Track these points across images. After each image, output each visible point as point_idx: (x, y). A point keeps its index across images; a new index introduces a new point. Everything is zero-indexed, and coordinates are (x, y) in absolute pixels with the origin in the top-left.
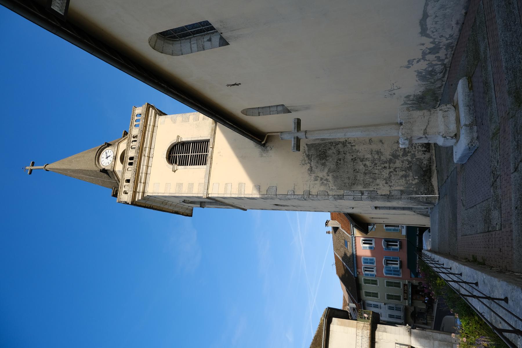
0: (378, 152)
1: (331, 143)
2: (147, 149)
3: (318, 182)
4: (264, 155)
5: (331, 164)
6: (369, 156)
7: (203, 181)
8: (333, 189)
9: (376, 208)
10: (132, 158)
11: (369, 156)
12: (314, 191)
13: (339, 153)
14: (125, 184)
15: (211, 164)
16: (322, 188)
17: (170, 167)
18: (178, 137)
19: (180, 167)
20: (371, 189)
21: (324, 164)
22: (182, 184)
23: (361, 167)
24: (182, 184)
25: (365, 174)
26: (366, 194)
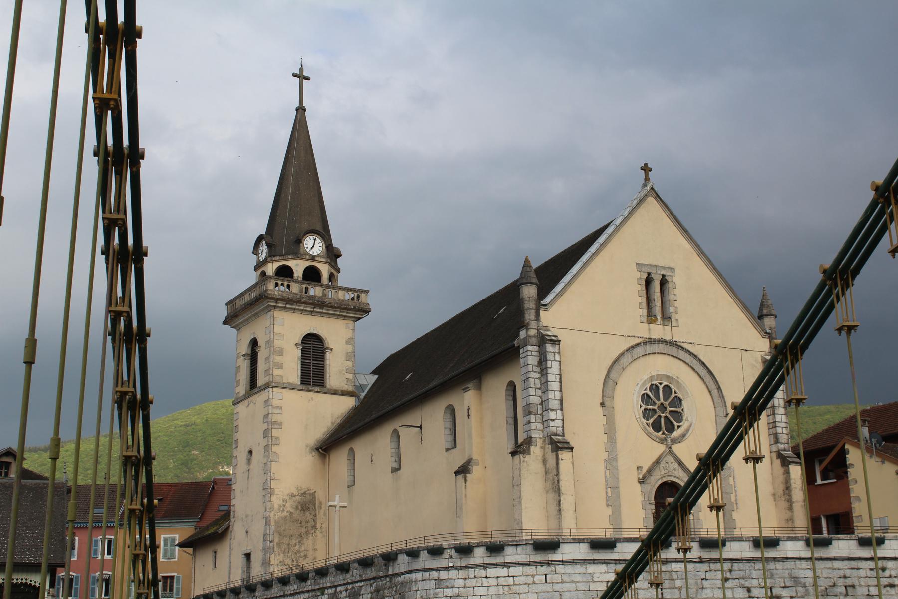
0: (306, 556)
1: (315, 515)
3: (281, 503)
5: (297, 514)
7: (285, 381)
8: (275, 516)
9: (248, 556)
12: (274, 498)
14: (286, 283)
16: (276, 506)
18: (331, 349)
19: (300, 351)
20: (276, 549)
21: (297, 508)
23: (294, 541)
25: (288, 544)
26: (271, 544)
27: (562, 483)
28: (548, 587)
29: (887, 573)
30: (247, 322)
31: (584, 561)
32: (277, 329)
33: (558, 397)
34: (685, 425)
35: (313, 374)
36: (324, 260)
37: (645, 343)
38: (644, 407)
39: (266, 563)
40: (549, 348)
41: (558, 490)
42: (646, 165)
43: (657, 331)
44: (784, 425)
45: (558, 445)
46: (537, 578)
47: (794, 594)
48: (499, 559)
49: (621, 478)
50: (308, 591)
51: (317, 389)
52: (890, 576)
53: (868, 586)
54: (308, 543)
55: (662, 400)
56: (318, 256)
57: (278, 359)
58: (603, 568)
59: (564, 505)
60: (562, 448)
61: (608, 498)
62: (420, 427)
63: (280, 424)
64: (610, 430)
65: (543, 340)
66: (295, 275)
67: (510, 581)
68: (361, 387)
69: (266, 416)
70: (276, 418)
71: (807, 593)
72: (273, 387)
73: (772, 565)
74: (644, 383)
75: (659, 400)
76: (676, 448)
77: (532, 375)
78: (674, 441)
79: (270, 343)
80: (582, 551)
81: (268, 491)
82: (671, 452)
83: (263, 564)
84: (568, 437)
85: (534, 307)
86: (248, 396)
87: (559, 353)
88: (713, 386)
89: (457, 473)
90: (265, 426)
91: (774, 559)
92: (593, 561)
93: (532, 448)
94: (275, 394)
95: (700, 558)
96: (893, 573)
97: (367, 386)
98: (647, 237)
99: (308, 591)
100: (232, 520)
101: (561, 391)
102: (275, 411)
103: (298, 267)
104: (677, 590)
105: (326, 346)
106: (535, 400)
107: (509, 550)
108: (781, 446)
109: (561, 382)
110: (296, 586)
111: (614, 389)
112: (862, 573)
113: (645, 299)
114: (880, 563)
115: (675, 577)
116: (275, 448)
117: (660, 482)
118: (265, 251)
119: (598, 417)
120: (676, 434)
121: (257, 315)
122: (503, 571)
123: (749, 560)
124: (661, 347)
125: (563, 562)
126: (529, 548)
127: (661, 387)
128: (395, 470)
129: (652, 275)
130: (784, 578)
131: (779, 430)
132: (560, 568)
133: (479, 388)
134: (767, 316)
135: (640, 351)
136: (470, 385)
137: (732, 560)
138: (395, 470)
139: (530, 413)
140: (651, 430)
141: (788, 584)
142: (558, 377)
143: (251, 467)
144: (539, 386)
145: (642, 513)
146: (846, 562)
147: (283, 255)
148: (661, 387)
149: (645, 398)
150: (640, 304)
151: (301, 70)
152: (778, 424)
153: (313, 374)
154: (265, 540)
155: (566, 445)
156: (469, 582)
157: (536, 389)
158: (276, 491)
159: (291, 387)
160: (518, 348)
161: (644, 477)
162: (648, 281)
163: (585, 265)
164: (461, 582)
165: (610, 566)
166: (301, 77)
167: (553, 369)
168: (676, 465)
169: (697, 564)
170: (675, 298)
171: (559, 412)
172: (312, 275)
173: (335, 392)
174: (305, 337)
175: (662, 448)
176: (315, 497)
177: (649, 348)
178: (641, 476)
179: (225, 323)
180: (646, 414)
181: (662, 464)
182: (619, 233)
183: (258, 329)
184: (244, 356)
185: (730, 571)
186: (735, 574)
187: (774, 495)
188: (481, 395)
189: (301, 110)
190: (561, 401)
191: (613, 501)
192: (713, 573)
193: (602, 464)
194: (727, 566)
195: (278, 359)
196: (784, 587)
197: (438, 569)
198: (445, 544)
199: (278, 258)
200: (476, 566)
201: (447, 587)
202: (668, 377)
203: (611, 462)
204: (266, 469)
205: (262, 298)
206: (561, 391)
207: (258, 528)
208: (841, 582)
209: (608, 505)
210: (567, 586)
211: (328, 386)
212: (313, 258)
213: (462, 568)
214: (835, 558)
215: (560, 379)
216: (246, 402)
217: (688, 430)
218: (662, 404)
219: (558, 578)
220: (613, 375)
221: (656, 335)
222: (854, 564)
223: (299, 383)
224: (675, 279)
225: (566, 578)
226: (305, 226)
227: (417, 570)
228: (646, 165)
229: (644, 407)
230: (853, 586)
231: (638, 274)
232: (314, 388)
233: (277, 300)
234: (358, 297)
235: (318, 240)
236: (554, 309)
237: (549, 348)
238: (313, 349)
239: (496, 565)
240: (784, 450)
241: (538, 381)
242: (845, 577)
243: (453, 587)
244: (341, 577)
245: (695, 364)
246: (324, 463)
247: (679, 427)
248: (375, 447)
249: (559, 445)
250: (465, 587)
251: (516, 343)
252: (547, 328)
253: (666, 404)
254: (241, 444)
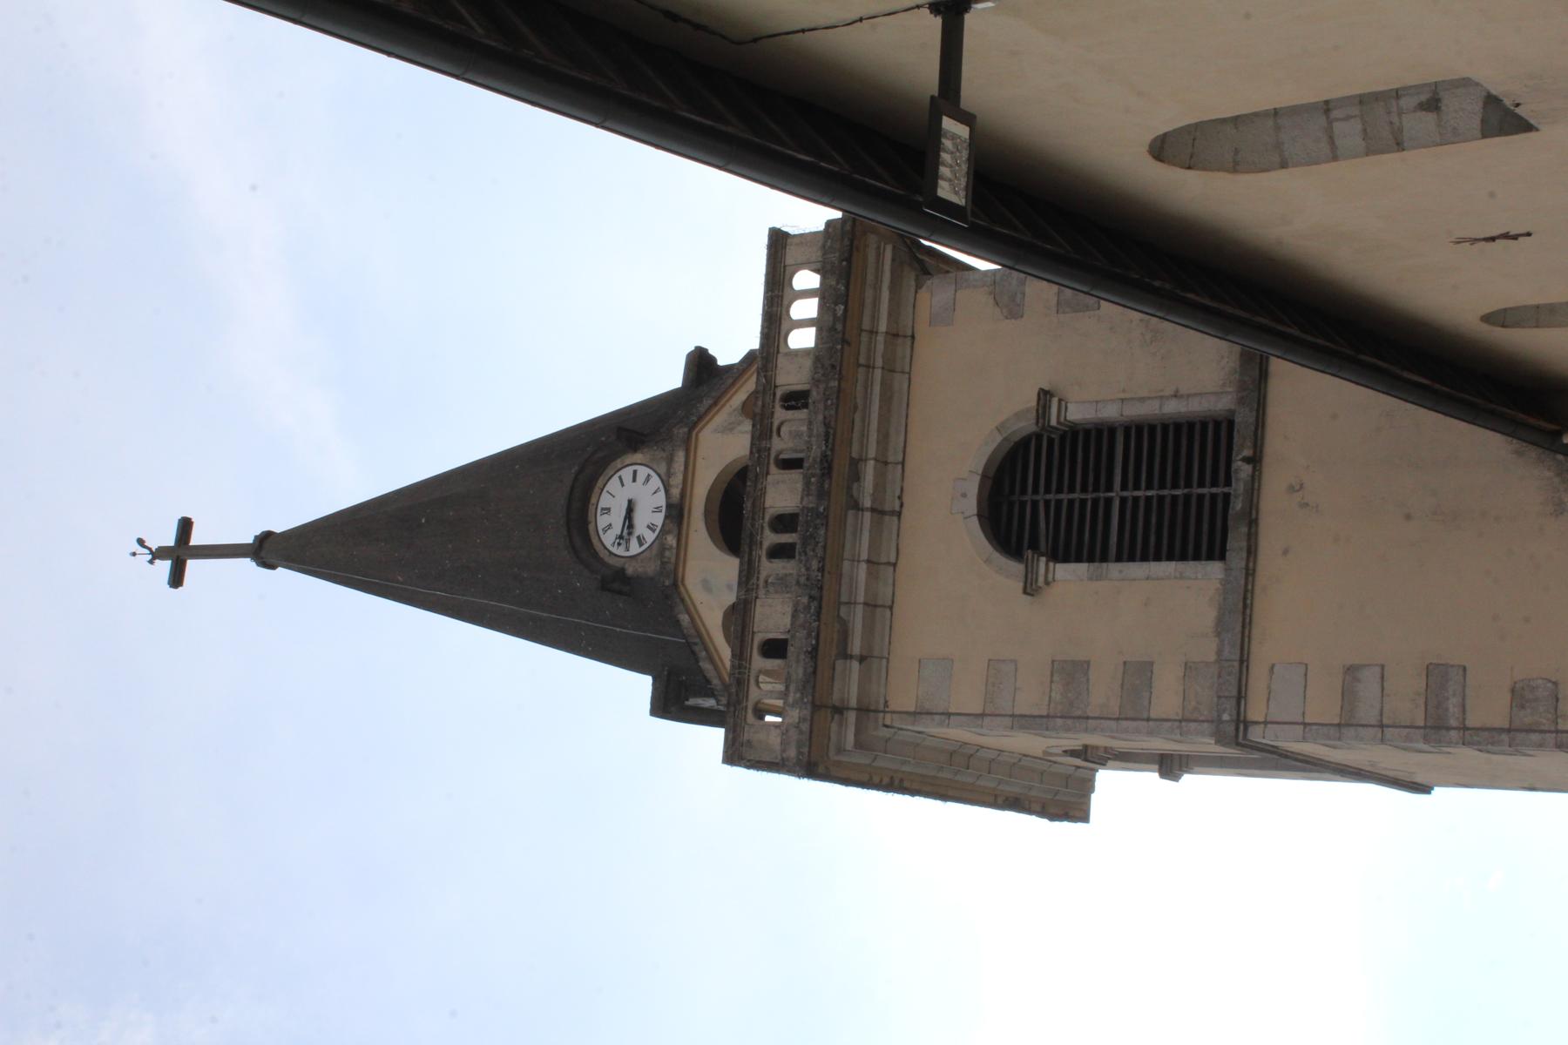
2: (869, 470)
7: (1207, 650)
10: (784, 522)
15: (1252, 552)
17: (1005, 574)
18: (1045, 396)
19: (1063, 571)
22: (1084, 666)
24: (1084, 666)
36: (680, 457)
105: (1028, 426)
151: (158, 554)
159: (1239, 614)
166: (180, 553)
189: (269, 550)
211: (1222, 404)
212: (676, 513)
223: (1215, 569)
232: (1238, 488)
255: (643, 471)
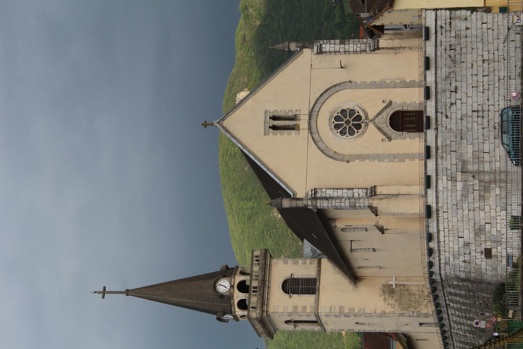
0: (422, 291)
2: (267, 282)
3: (390, 306)
4: (356, 289)
5: (397, 297)
6: (417, 293)
7: (314, 305)
8: (398, 310)
10: (254, 288)
11: (417, 293)
12: (387, 311)
13: (401, 290)
16: (392, 310)
17: (287, 296)
18: (292, 274)
19: (294, 295)
20: (418, 310)
21: (393, 296)
22: (297, 307)
23: (413, 299)
24: (297, 307)
25: (415, 302)
26: (415, 313)
27: (394, 193)
28: (450, 211)
29: (444, 25)
30: (273, 325)
31: (436, 192)
32: (281, 310)
33: (345, 191)
34: (357, 109)
35: (307, 286)
36: (233, 279)
37: (311, 133)
38: (347, 134)
39: (426, 315)
40: (319, 195)
41: (397, 195)
42: (203, 125)
43: (303, 123)
44: (355, 46)
45: (372, 192)
46: (445, 217)
47: (454, 79)
48: (435, 235)
49: (388, 152)
50: (447, 310)
51: (318, 284)
52: (445, 24)
53: (450, 37)
54: (414, 290)
55: (343, 122)
56: (230, 283)
57: (300, 310)
58: (440, 182)
59: (406, 193)
60: (375, 192)
61: (400, 161)
62: (351, 241)
63: (341, 307)
64: (362, 157)
65: (315, 198)
66: (244, 298)
67: (446, 230)
68: (313, 251)
69: (336, 316)
70: (337, 310)
71: (454, 72)
72: (318, 313)
73: (439, 90)
74: (333, 132)
75: (343, 124)
76: (371, 117)
77: (333, 204)
78: (367, 118)
79: (289, 314)
80: (431, 193)
81: (383, 314)
82: (372, 120)
83: (427, 317)
84: (369, 187)
85: (295, 201)
86: (321, 325)
87: (321, 189)
88: (334, 90)
89: (383, 233)
90: (342, 317)
91: (436, 88)
92: (436, 187)
93: (374, 206)
94: (323, 310)
95: (435, 129)
96: (444, 22)
97: (312, 247)
98: (246, 124)
99: (447, 310)
100: (398, 332)
101: (342, 189)
102: (333, 311)
103: (238, 296)
104: (452, 143)
105: (289, 277)
106: (347, 203)
107: (431, 230)
108: (368, 49)
109: (337, 189)
110: (444, 314)
111: (339, 154)
112: (443, 40)
113: (285, 131)
114: (439, 29)
115: (444, 144)
116: (356, 311)
117: (390, 127)
118: (227, 316)
119: (355, 164)
120: (362, 114)
121: (270, 321)
122: (442, 233)
123: (436, 103)
124: (313, 122)
125: (437, 203)
126: (430, 220)
127: (336, 123)
128: (366, 230)
129: (271, 125)
130: (446, 84)
131: (358, 49)
132: (440, 204)
133: (334, 220)
134: (289, 48)
135: (316, 136)
136: (333, 225)
137: (436, 112)
138: (366, 230)
139: (355, 206)
140: (360, 131)
141: (449, 82)
142: (335, 190)
143: (366, 323)
144: (340, 200)
145: (408, 140)
146: (438, 48)
147: (231, 306)
148: (336, 123)
149: (342, 133)
150: (288, 134)
151: (99, 292)
152: (355, 50)
153: (307, 286)
154: (413, 317)
155: (373, 190)
156: (447, 250)
157: (341, 202)
158: (383, 310)
159: (317, 301)
160: (318, 209)
161: (388, 138)
162: (274, 128)
163: (268, 169)
164: (447, 254)
165: (439, 178)
166: (104, 292)
167: (330, 193)
168: (380, 116)
169: (439, 131)
170: (283, 111)
171: (354, 191)
172: (243, 287)
173: (319, 272)
174: (284, 292)
175: (371, 125)
176: (386, 285)
177: (314, 130)
178: (387, 140)
179: (272, 338)
180: (352, 133)
181: (380, 125)
182: (247, 145)
183: (279, 322)
184: (295, 327)
185: (442, 113)
186: (444, 111)
187: (395, 53)
188: (338, 219)
189: (128, 292)
190: (348, 189)
191: (401, 157)
192: (443, 123)
193: (381, 163)
194: (439, 115)
195: (300, 310)
196: (451, 84)
197: (440, 264)
198: (427, 260)
199: (233, 309)
200: (439, 246)
201: (449, 260)
202: (331, 117)
203: (380, 158)
204: (370, 315)
205: (262, 321)
206: (342, 189)
207: (405, 320)
208: (448, 52)
209: (404, 161)
210: (449, 201)
211: (315, 277)
212: (232, 286)
213: (439, 253)
214: (436, 54)
215: (336, 189)
216: (325, 326)
217: (360, 108)
218: (345, 122)
219: (445, 206)
220: (331, 154)
221: (306, 126)
222: (439, 44)
223: (314, 295)
224: (272, 111)
225: (445, 202)
226: (210, 291)
227: (440, 272)
228: (203, 125)
229: (347, 134)
230: (451, 45)
231: (271, 135)
232: (317, 286)
233: (263, 311)
234: (256, 257)
235: (220, 283)
236: (295, 189)
237: (319, 195)
238: (292, 286)
239: (438, 237)
240: (370, 47)
241: (337, 201)
242: (446, 50)
243: (449, 257)
244: (440, 298)
245: (321, 101)
246: (364, 279)
247: (358, 112)
248: (358, 259)
249: (372, 192)
250: (449, 252)
251: (315, 211)
252: (307, 194)
253: (345, 120)
254: (351, 328)
255: (225, 281)
